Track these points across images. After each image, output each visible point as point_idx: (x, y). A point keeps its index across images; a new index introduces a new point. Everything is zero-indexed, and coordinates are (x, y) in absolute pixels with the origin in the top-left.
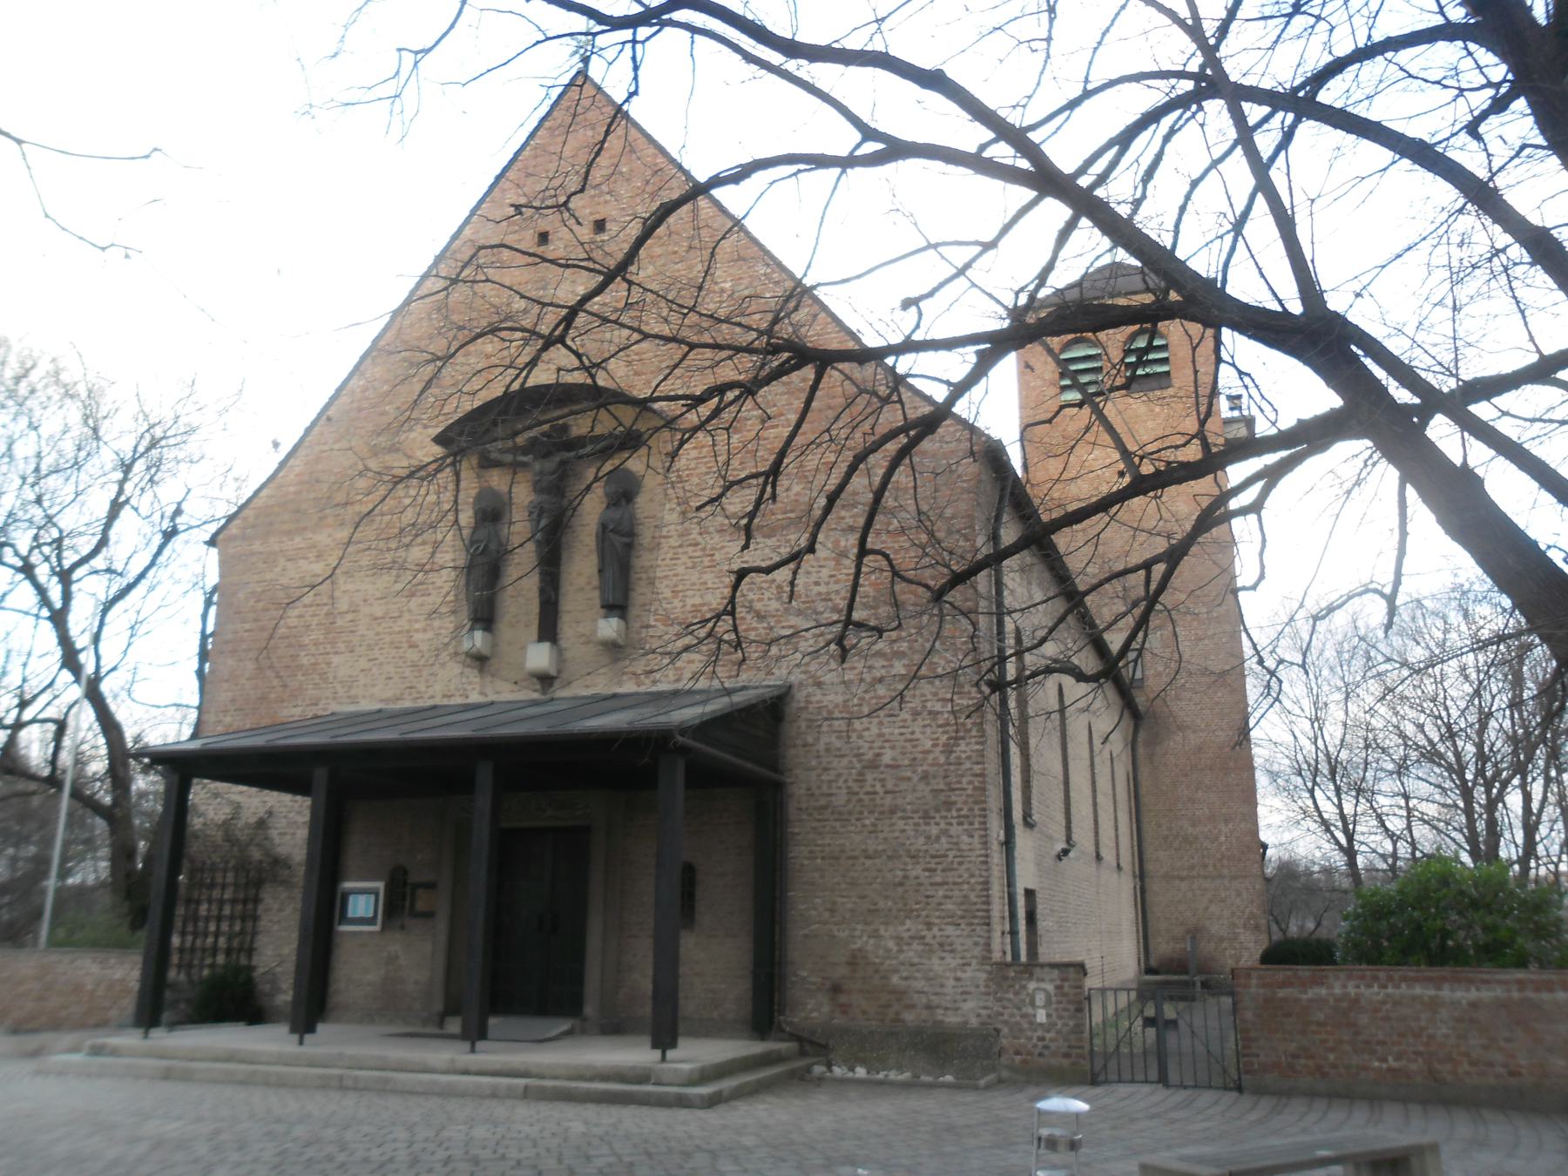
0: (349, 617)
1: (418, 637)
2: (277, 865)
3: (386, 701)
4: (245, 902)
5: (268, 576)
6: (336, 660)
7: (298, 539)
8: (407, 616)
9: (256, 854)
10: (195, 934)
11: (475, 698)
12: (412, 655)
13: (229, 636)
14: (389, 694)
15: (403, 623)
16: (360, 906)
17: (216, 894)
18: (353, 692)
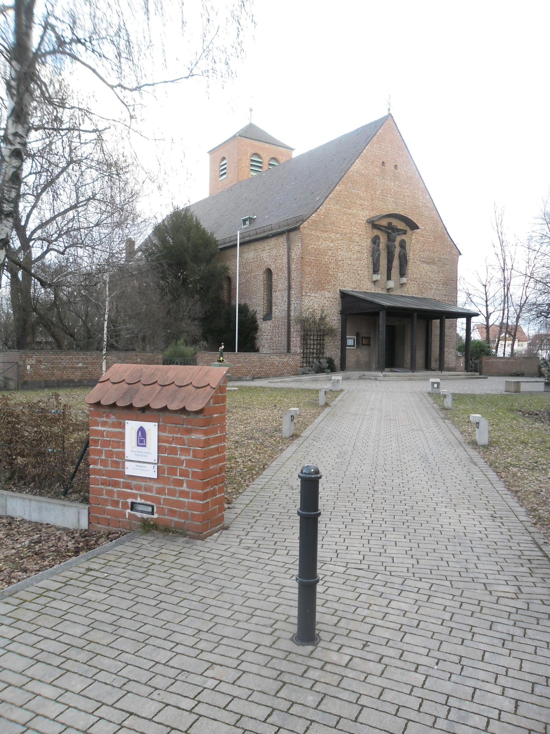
0: (342, 262)
1: (359, 272)
2: (331, 332)
3: (353, 288)
4: (320, 340)
5: (317, 244)
6: (339, 274)
7: (325, 234)
8: (356, 266)
9: (322, 327)
10: (307, 349)
11: (373, 291)
12: (358, 277)
13: (308, 260)
14: (353, 287)
15: (355, 268)
16: (350, 342)
17: (312, 337)
18: (344, 284)
